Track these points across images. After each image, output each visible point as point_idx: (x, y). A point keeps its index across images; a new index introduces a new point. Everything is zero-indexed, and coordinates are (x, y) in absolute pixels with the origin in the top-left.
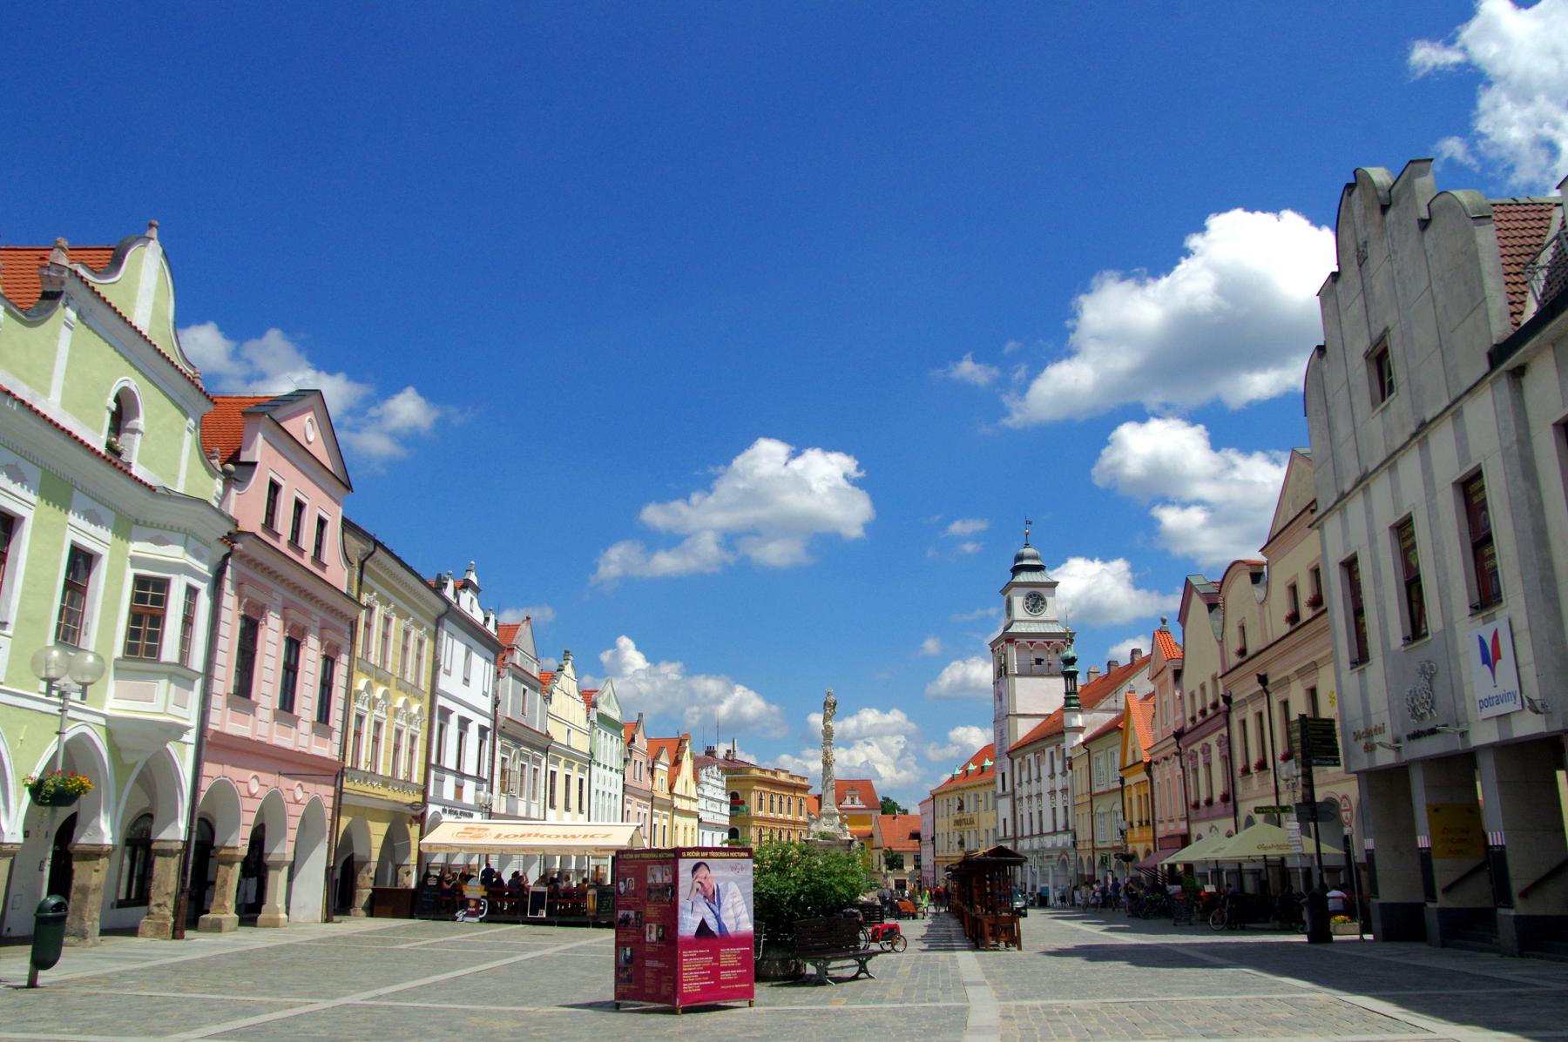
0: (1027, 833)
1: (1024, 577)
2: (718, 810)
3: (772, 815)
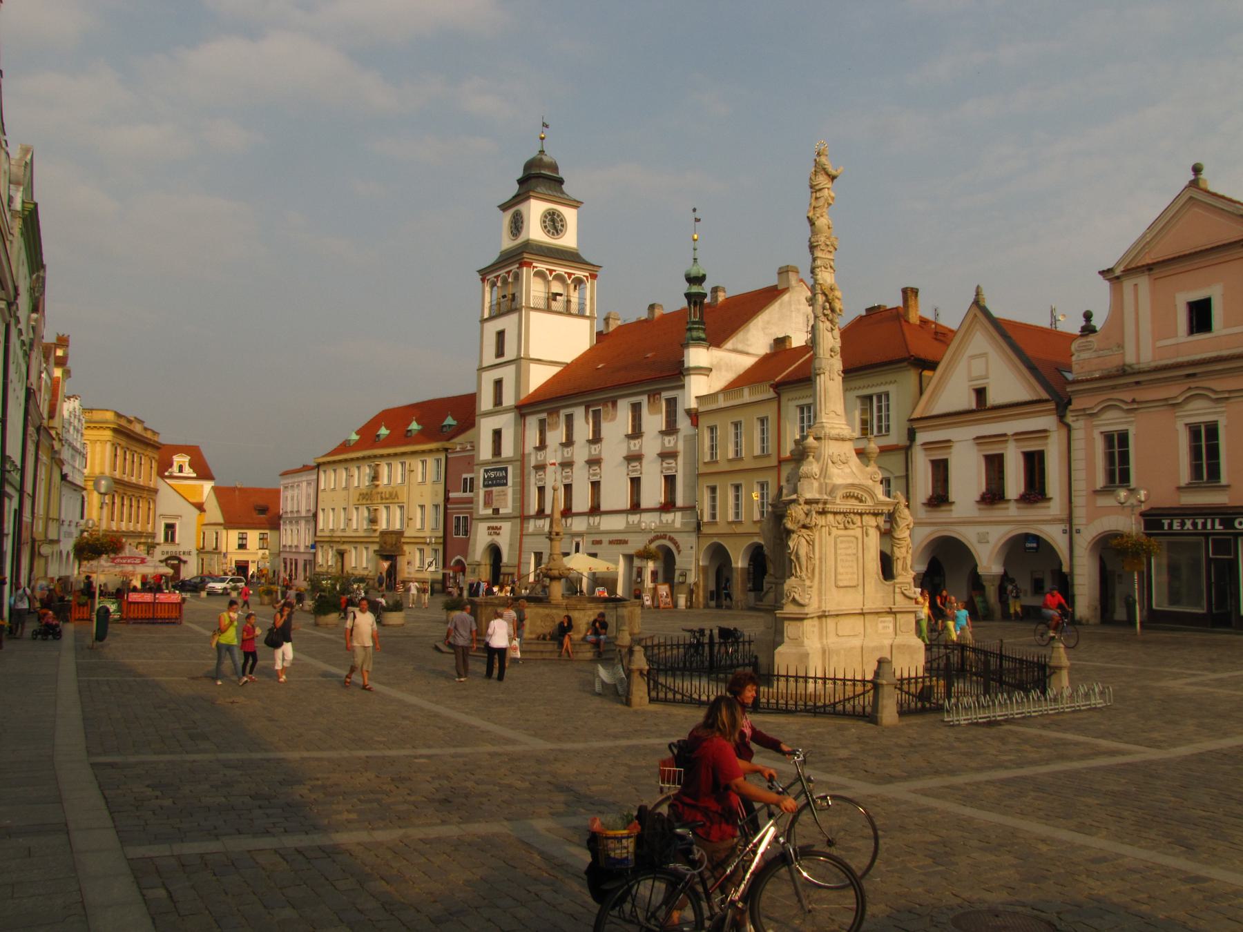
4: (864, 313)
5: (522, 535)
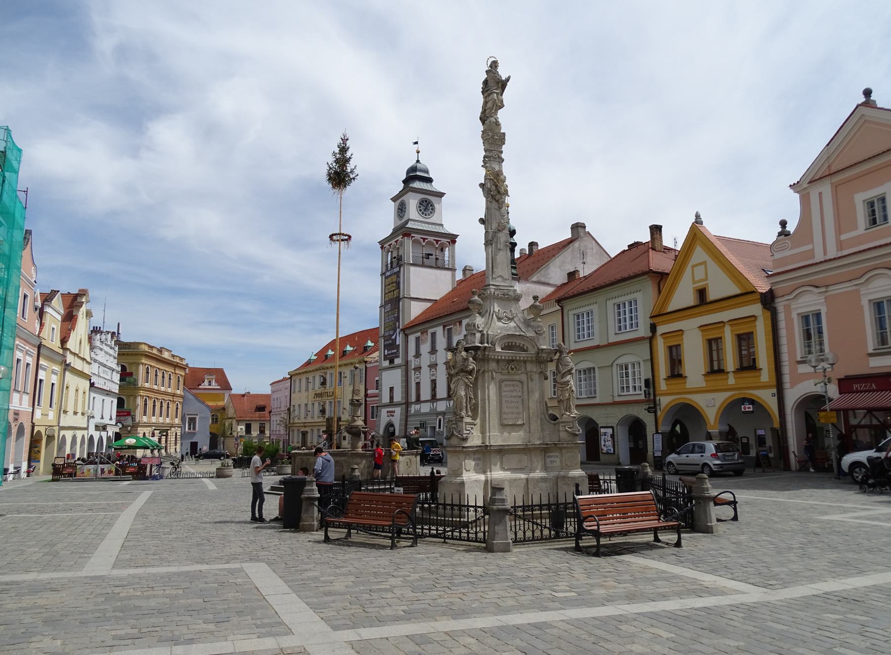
0: (426, 394)
1: (417, 185)
2: (109, 377)
3: (155, 387)
4: (627, 248)
5: (407, 417)
